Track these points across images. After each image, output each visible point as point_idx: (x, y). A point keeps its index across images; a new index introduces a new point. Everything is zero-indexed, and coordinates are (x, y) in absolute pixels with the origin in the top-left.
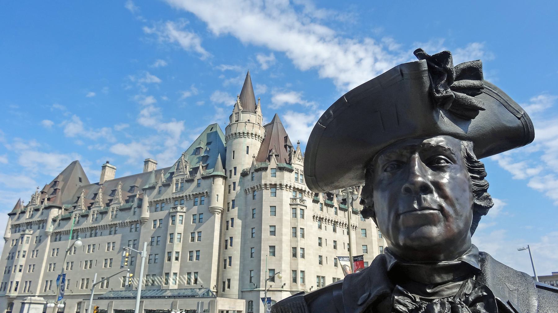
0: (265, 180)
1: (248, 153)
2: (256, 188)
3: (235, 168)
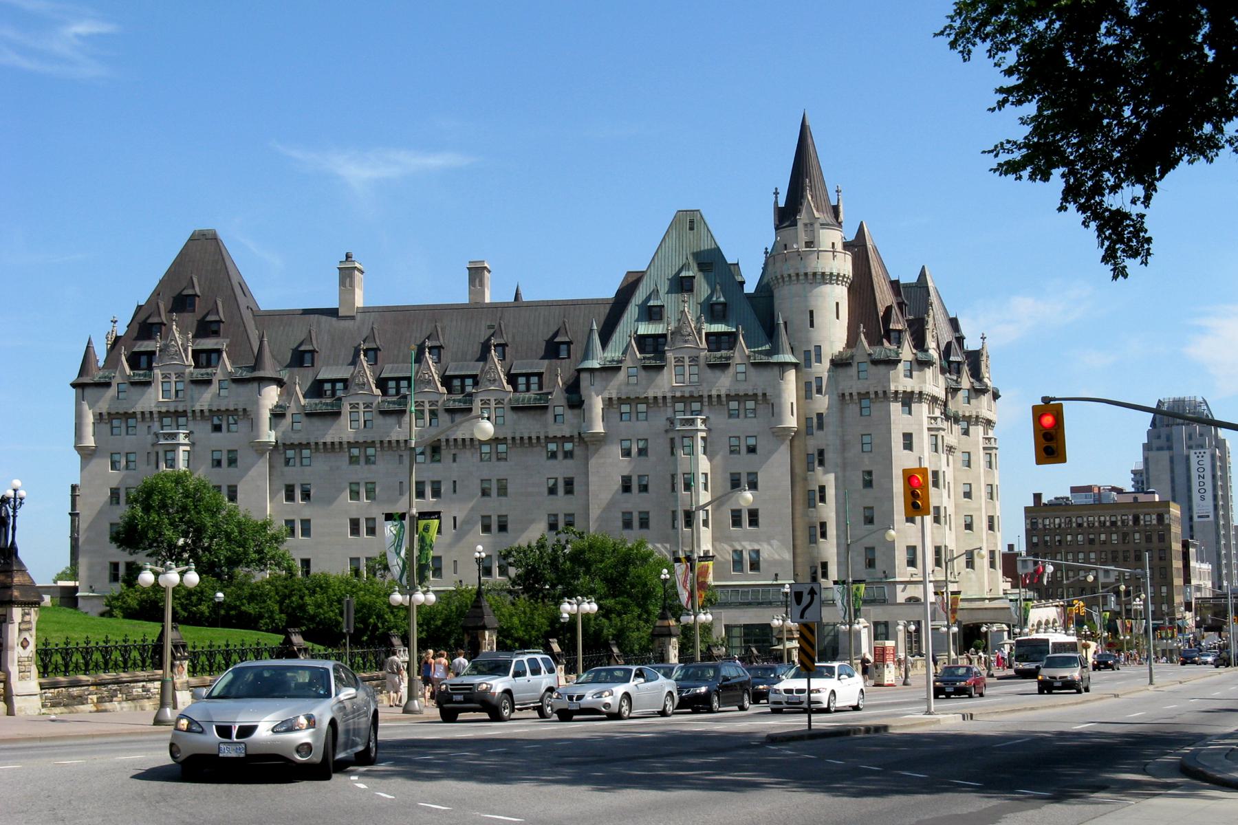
0: (895, 384)
1: (838, 318)
2: (872, 396)
3: (818, 348)
